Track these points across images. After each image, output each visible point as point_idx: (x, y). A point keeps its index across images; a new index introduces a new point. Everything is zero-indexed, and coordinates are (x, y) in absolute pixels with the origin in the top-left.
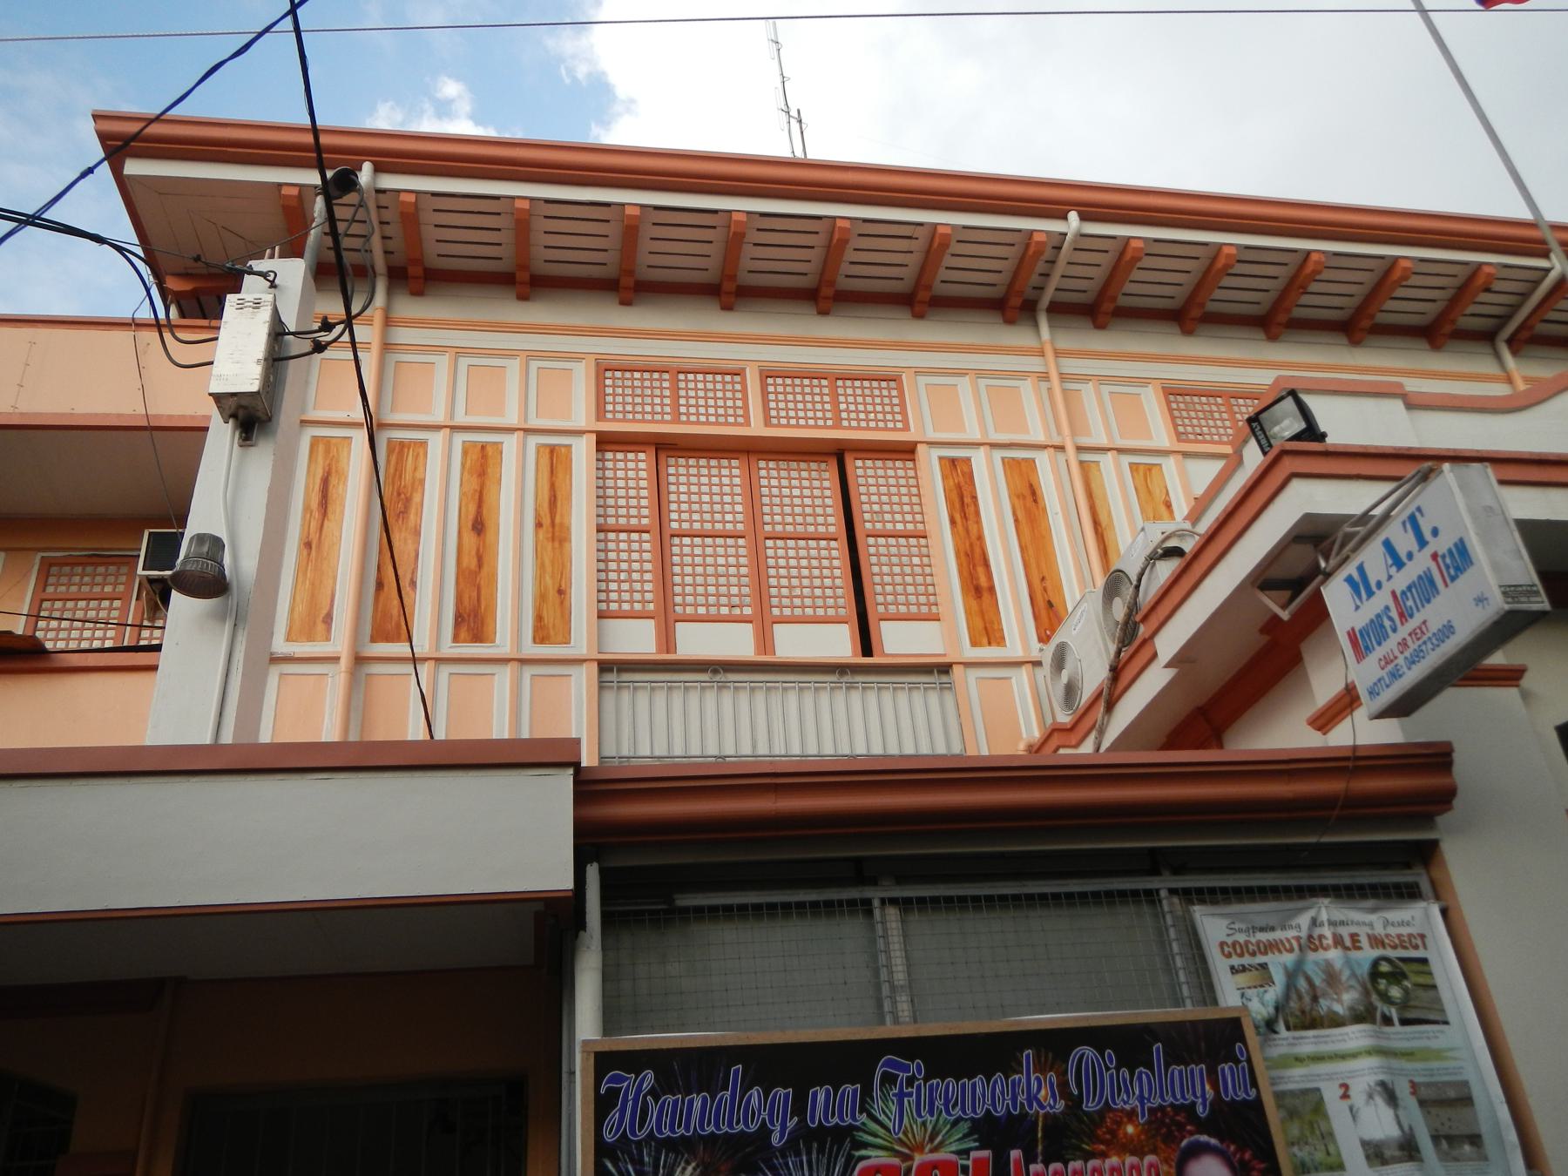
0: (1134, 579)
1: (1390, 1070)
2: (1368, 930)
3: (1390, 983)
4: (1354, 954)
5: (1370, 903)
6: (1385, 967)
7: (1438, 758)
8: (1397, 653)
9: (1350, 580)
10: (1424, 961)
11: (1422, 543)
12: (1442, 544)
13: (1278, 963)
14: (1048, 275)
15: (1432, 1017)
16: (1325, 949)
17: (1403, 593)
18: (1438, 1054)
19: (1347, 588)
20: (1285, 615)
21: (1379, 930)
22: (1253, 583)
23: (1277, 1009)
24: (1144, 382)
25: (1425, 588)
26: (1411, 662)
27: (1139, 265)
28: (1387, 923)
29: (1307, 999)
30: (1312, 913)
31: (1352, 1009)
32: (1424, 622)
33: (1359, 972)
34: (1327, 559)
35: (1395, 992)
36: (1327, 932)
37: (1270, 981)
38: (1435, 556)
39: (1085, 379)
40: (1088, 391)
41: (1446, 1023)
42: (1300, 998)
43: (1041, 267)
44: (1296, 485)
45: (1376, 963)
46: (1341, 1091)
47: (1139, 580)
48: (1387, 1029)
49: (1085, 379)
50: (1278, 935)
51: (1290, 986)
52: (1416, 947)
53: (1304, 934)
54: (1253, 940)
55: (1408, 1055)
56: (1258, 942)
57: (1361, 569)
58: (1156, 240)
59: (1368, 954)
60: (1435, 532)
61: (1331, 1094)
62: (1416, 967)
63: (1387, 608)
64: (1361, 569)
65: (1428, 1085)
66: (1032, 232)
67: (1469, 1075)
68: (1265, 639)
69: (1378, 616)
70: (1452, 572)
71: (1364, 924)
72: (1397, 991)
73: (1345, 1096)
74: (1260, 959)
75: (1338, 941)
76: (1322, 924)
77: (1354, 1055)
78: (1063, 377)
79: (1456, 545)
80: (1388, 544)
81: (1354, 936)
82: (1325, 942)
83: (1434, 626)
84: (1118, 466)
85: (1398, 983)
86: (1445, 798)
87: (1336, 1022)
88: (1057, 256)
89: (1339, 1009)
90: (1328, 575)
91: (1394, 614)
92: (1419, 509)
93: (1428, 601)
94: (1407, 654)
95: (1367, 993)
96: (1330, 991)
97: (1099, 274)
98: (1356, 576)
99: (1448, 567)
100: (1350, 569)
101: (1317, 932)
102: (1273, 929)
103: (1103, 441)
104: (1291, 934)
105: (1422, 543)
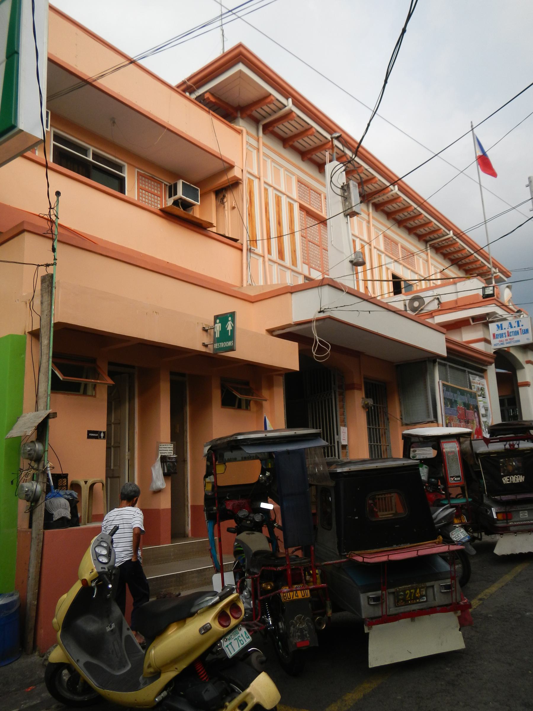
9: (498, 325)
11: (519, 326)
12: (523, 328)
25: (517, 333)
26: (507, 343)
60: (522, 326)
64: (501, 325)
91: (507, 334)
98: (500, 325)
105: (519, 326)
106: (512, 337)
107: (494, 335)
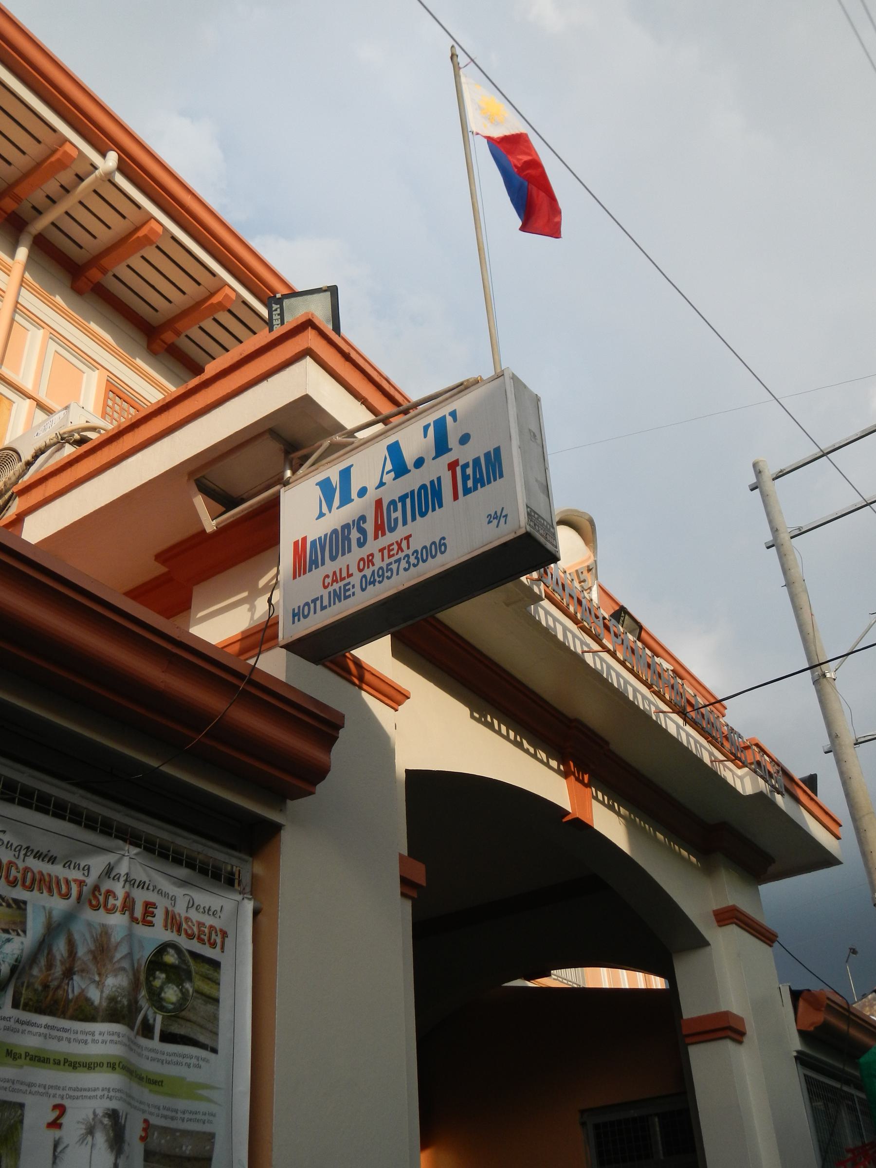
0: (27, 456)
1: (128, 1098)
2: (167, 903)
3: (168, 980)
4: (141, 931)
5: (183, 872)
6: (171, 958)
7: (325, 726)
8: (353, 569)
9: (326, 486)
10: (216, 965)
11: (441, 446)
13: (42, 906)
14: (54, 202)
15: (202, 1039)
16: (111, 911)
17: (393, 503)
18: (192, 1090)
19: (318, 492)
20: (210, 525)
21: (180, 909)
22: (191, 474)
23: (14, 969)
24: (94, 364)
25: (427, 499)
26: (368, 582)
27: (143, 252)
28: (191, 905)
29: (58, 970)
30: (111, 858)
31: (112, 999)
32: (407, 538)
33: (137, 956)
34: (294, 473)
35: (171, 994)
36: (119, 890)
37: (21, 927)
38: (452, 466)
39: (39, 323)
40: (35, 337)
41: (214, 1051)
42: (50, 966)
43: (52, 187)
44: (308, 362)
45: (163, 949)
46: (52, 1116)
47: (36, 457)
48: (143, 1042)
49: (39, 323)
50: (57, 870)
51: (44, 944)
52: (213, 945)
53: (91, 881)
54: (21, 865)
55: (155, 1082)
56: (27, 870)
57: (346, 474)
58: (174, 238)
59: (158, 934)
60: (465, 439)
61: (37, 1114)
62: (205, 969)
63: (363, 518)
65: (165, 1130)
66: (66, 140)
67: (218, 1128)
68: (161, 569)
69: (346, 527)
70: (470, 484)
71: (166, 895)
72: (171, 996)
73: (55, 1124)
74: (19, 893)
75: (128, 905)
76: (117, 878)
77: (90, 1066)
78: (17, 306)
79: (488, 455)
80: (394, 450)
81: (149, 906)
82: (111, 901)
83: (417, 544)
84: (31, 417)
85: (179, 984)
86: (313, 775)
87: (85, 1012)
88: (78, 185)
89: (95, 995)
90: (286, 483)
91: (369, 527)
92: (453, 414)
93: (423, 514)
94: (368, 572)
95: (135, 985)
96: (92, 967)
97: (105, 237)
99: (465, 478)
100: (333, 473)
101: (106, 885)
102: (53, 860)
103: (28, 385)
104: (74, 875)
106: (401, 532)
107: (299, 548)
